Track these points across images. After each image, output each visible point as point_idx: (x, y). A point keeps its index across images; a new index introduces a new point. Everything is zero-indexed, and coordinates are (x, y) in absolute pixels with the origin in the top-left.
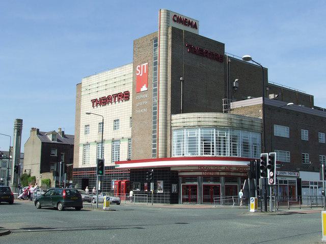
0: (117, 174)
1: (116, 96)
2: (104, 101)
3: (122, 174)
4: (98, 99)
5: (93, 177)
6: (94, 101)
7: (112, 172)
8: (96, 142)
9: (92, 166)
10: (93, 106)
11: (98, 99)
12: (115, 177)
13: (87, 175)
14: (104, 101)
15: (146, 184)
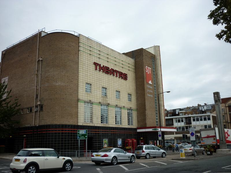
0: (121, 134)
1: (117, 72)
2: (107, 70)
3: (124, 134)
4: (102, 66)
5: (98, 136)
6: (96, 64)
7: (117, 132)
8: (100, 103)
9: (96, 125)
10: (96, 69)
11: (102, 66)
12: (119, 136)
13: (91, 134)
14: (107, 70)
15: (155, 141)
